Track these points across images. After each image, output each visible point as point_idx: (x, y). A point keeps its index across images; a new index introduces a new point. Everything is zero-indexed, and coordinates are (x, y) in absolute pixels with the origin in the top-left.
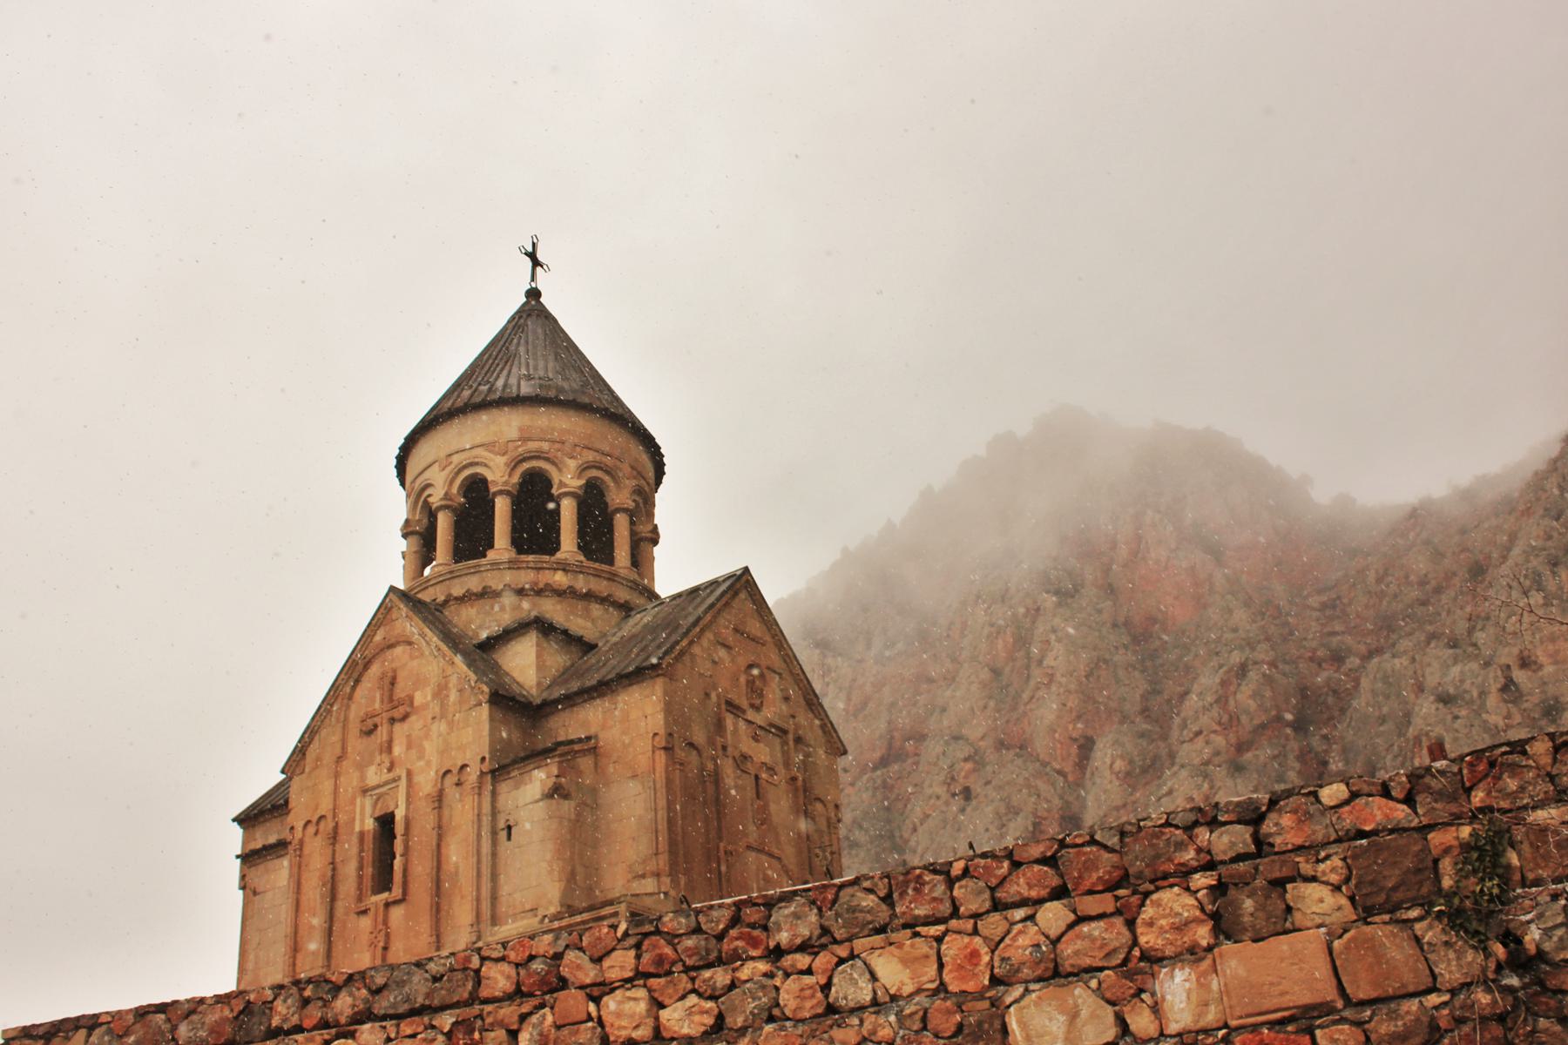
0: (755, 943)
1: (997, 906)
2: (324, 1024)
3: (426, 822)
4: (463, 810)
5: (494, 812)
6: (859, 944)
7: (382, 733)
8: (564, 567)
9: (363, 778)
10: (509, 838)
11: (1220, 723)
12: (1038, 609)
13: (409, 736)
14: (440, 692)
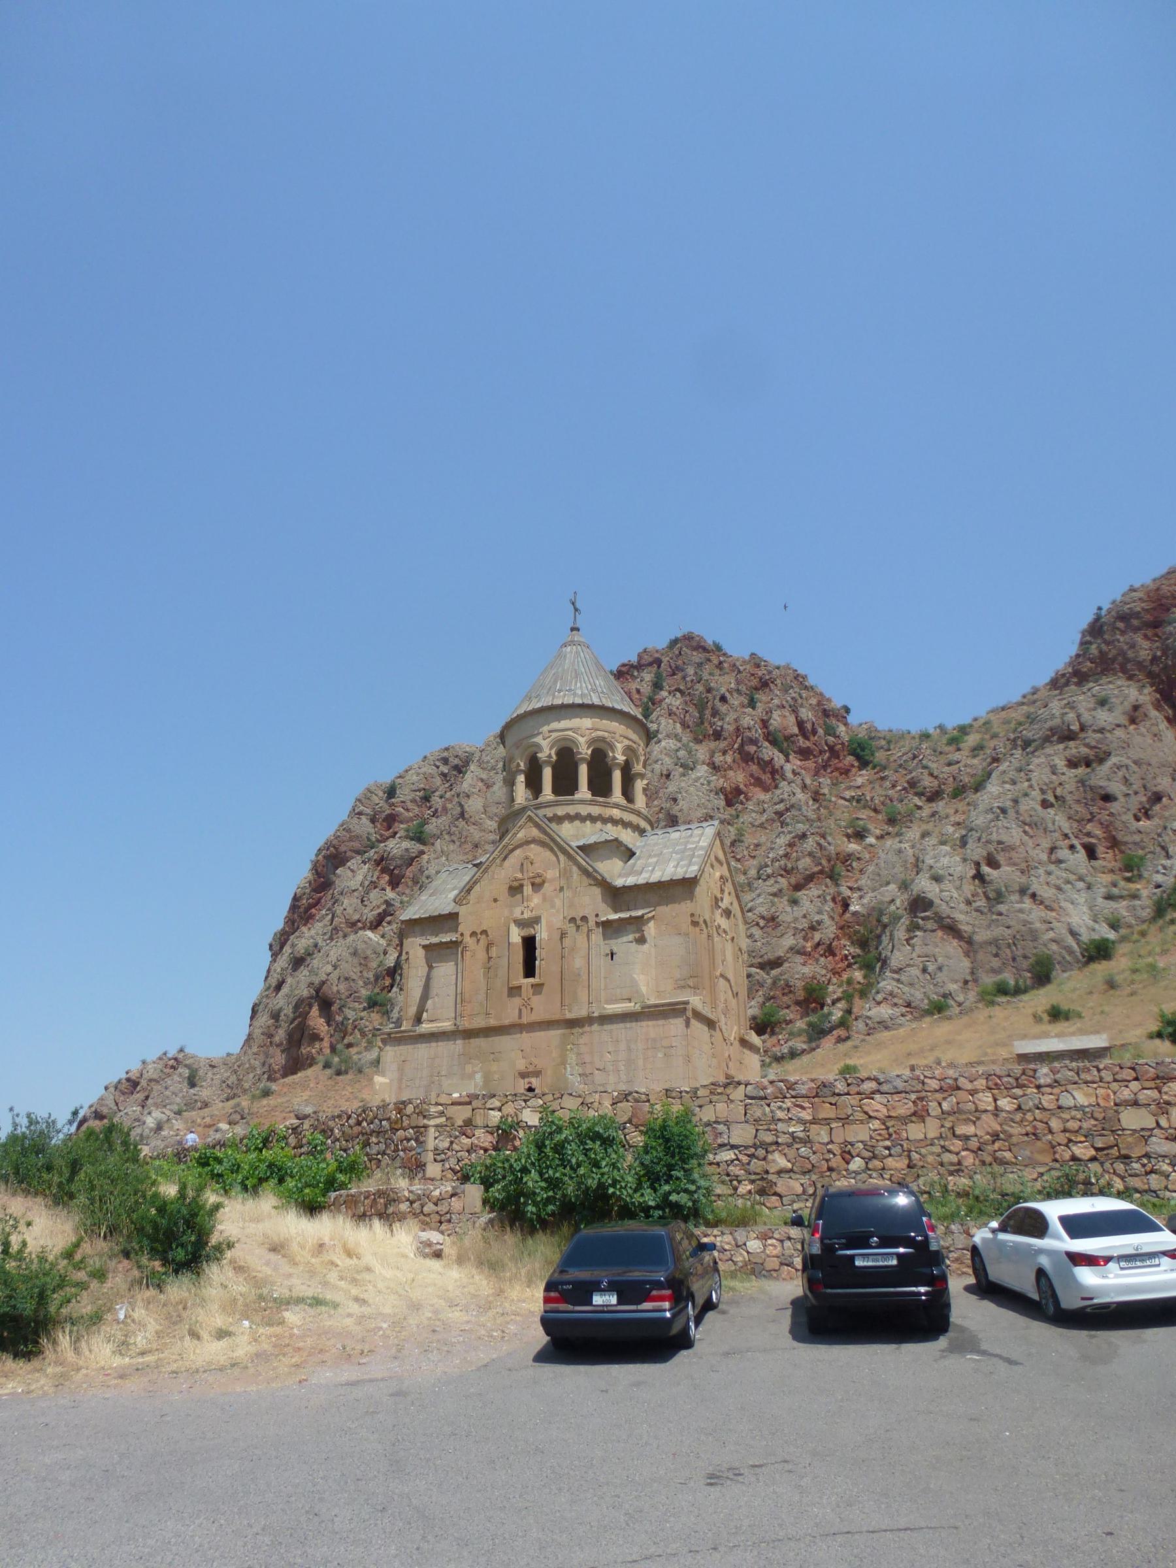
0: (1031, 1082)
1: (1115, 1080)
2: (858, 1093)
6: (1070, 1087)
8: (617, 806)
9: (511, 912)
11: (785, 870)
12: (668, 776)
14: (565, 874)
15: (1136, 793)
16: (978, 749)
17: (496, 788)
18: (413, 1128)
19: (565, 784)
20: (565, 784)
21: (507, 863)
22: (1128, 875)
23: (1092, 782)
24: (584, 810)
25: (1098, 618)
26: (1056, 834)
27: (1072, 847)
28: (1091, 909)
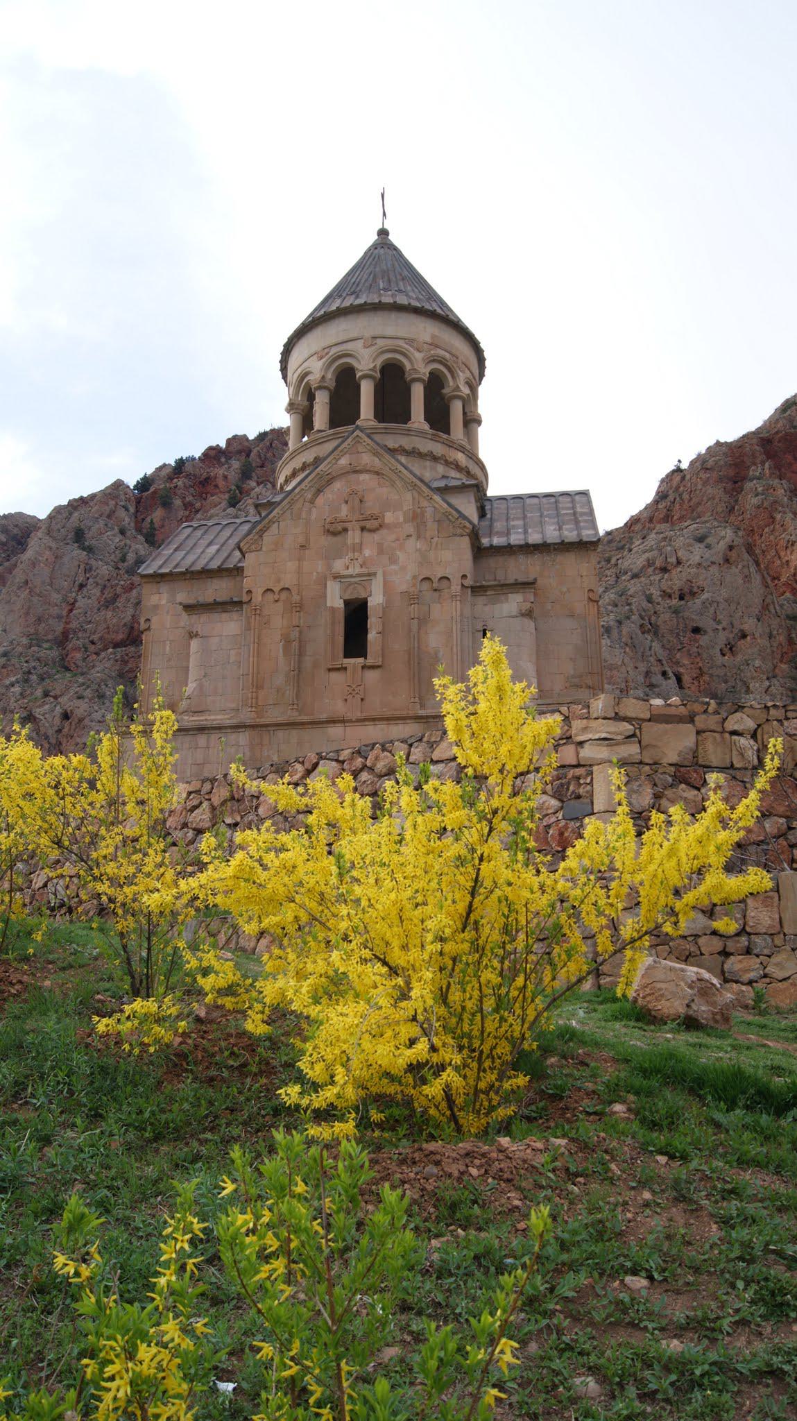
9: (329, 567)
14: (417, 518)
17: (66, 559)
21: (320, 500)
23: (686, 614)
24: (426, 446)
26: (652, 659)
27: (664, 674)
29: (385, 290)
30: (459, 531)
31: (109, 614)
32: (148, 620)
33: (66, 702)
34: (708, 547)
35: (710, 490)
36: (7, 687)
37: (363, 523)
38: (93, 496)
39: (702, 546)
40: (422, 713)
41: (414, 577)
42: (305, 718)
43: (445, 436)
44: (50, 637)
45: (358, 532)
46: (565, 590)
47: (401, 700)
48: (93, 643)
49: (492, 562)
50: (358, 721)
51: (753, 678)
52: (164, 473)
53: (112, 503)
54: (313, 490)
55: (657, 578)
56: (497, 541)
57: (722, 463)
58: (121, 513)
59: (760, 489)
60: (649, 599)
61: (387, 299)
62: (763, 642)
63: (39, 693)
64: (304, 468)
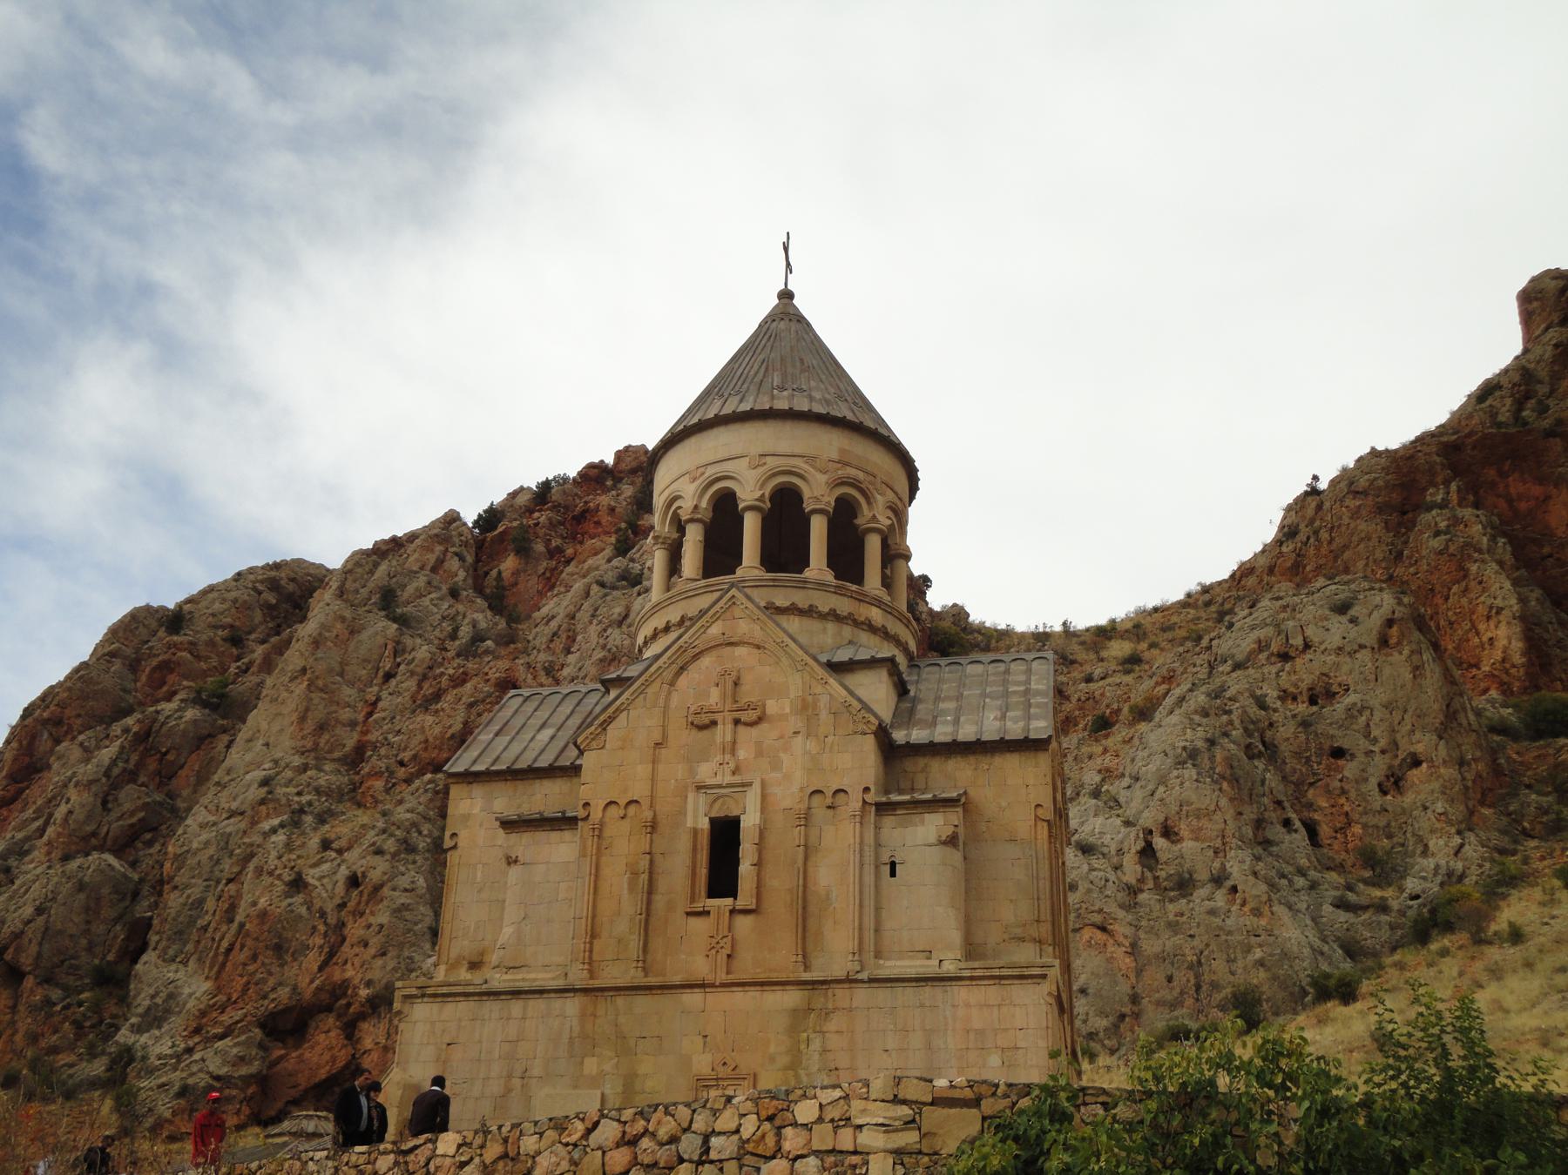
3: (786, 839)
4: (841, 837)
5: (878, 845)
7: (723, 732)
8: (878, 603)
9: (692, 772)
10: (893, 874)
13: (759, 744)
14: (806, 708)
15: (1383, 752)
16: (1133, 660)
17: (364, 636)
18: (817, 1153)
19: (785, 551)
20: (785, 551)
21: (683, 681)
22: (1367, 874)
23: (1320, 728)
24: (825, 602)
25: (1313, 492)
26: (1266, 800)
27: (1287, 823)
28: (1313, 920)
29: (782, 389)
30: (862, 727)
31: (429, 719)
32: (454, 835)
33: (356, 859)
34: (1354, 621)
35: (1363, 526)
36: (266, 835)
37: (737, 715)
38: (412, 537)
39: (1344, 619)
40: (806, 976)
41: (802, 789)
42: (653, 980)
43: (854, 587)
44: (337, 754)
45: (730, 726)
46: (1004, 804)
47: (782, 960)
48: (401, 764)
49: (911, 765)
50: (723, 985)
51: (1432, 832)
52: (522, 500)
53: (439, 548)
54: (675, 667)
55: (1274, 669)
56: (918, 735)
57: (1381, 483)
58: (453, 564)
59: (1443, 525)
60: (1262, 705)
61: (782, 404)
62: (1448, 772)
63: (314, 842)
64: (667, 629)
